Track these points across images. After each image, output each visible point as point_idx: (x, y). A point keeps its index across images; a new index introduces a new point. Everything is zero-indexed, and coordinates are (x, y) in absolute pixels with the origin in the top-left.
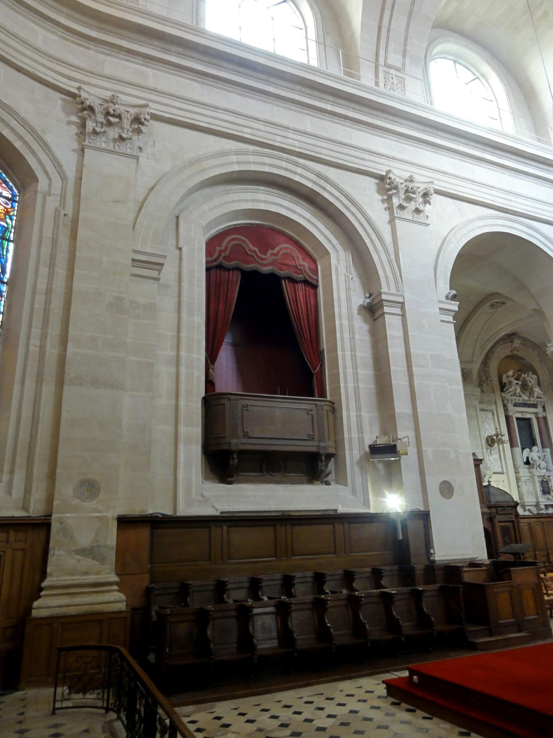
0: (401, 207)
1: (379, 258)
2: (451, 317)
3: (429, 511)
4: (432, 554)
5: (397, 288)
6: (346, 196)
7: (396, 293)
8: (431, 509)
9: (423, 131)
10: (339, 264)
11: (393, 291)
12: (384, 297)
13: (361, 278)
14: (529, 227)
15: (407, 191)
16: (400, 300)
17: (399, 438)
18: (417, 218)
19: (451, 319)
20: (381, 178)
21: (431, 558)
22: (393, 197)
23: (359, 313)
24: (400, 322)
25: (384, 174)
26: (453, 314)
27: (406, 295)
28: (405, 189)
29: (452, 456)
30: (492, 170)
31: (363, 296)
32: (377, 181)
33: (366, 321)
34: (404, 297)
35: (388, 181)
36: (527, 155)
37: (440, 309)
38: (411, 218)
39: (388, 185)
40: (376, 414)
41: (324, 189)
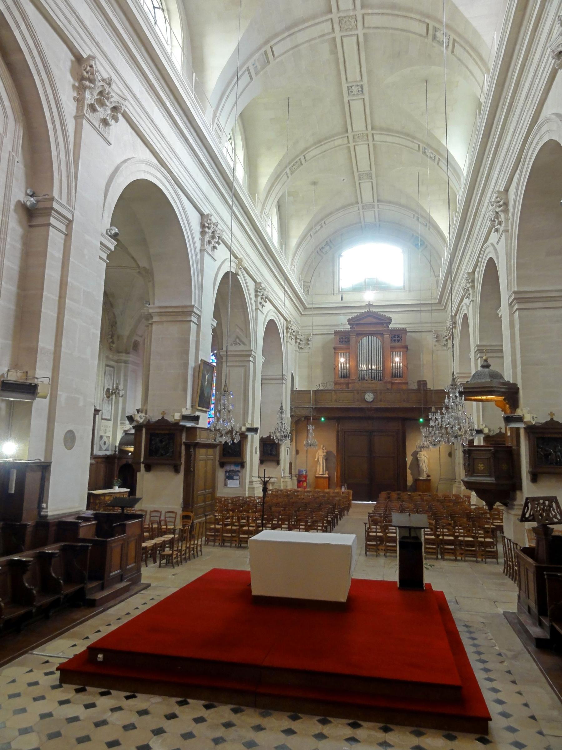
0: (92, 108)
1: (58, 154)
2: (106, 255)
3: (51, 463)
4: (43, 508)
5: (69, 200)
6: (40, 53)
7: (65, 204)
8: (53, 460)
9: (129, 35)
10: (6, 135)
11: (64, 202)
12: (55, 206)
13: (25, 166)
14: (176, 192)
15: (101, 93)
16: (70, 217)
17: (37, 376)
18: (102, 129)
19: (105, 256)
20: (78, 59)
21: (42, 513)
22: (87, 90)
23: (15, 211)
24: (63, 242)
25: (85, 56)
26: (109, 252)
27: (76, 213)
28: (100, 89)
29: (81, 404)
30: (165, 118)
31: (23, 190)
32: (73, 58)
33: (20, 222)
34: (73, 215)
35: (88, 68)
36: (194, 124)
37: (101, 243)
38: (97, 127)
39: (87, 72)
40: (10, 342)
41: (18, 27)
